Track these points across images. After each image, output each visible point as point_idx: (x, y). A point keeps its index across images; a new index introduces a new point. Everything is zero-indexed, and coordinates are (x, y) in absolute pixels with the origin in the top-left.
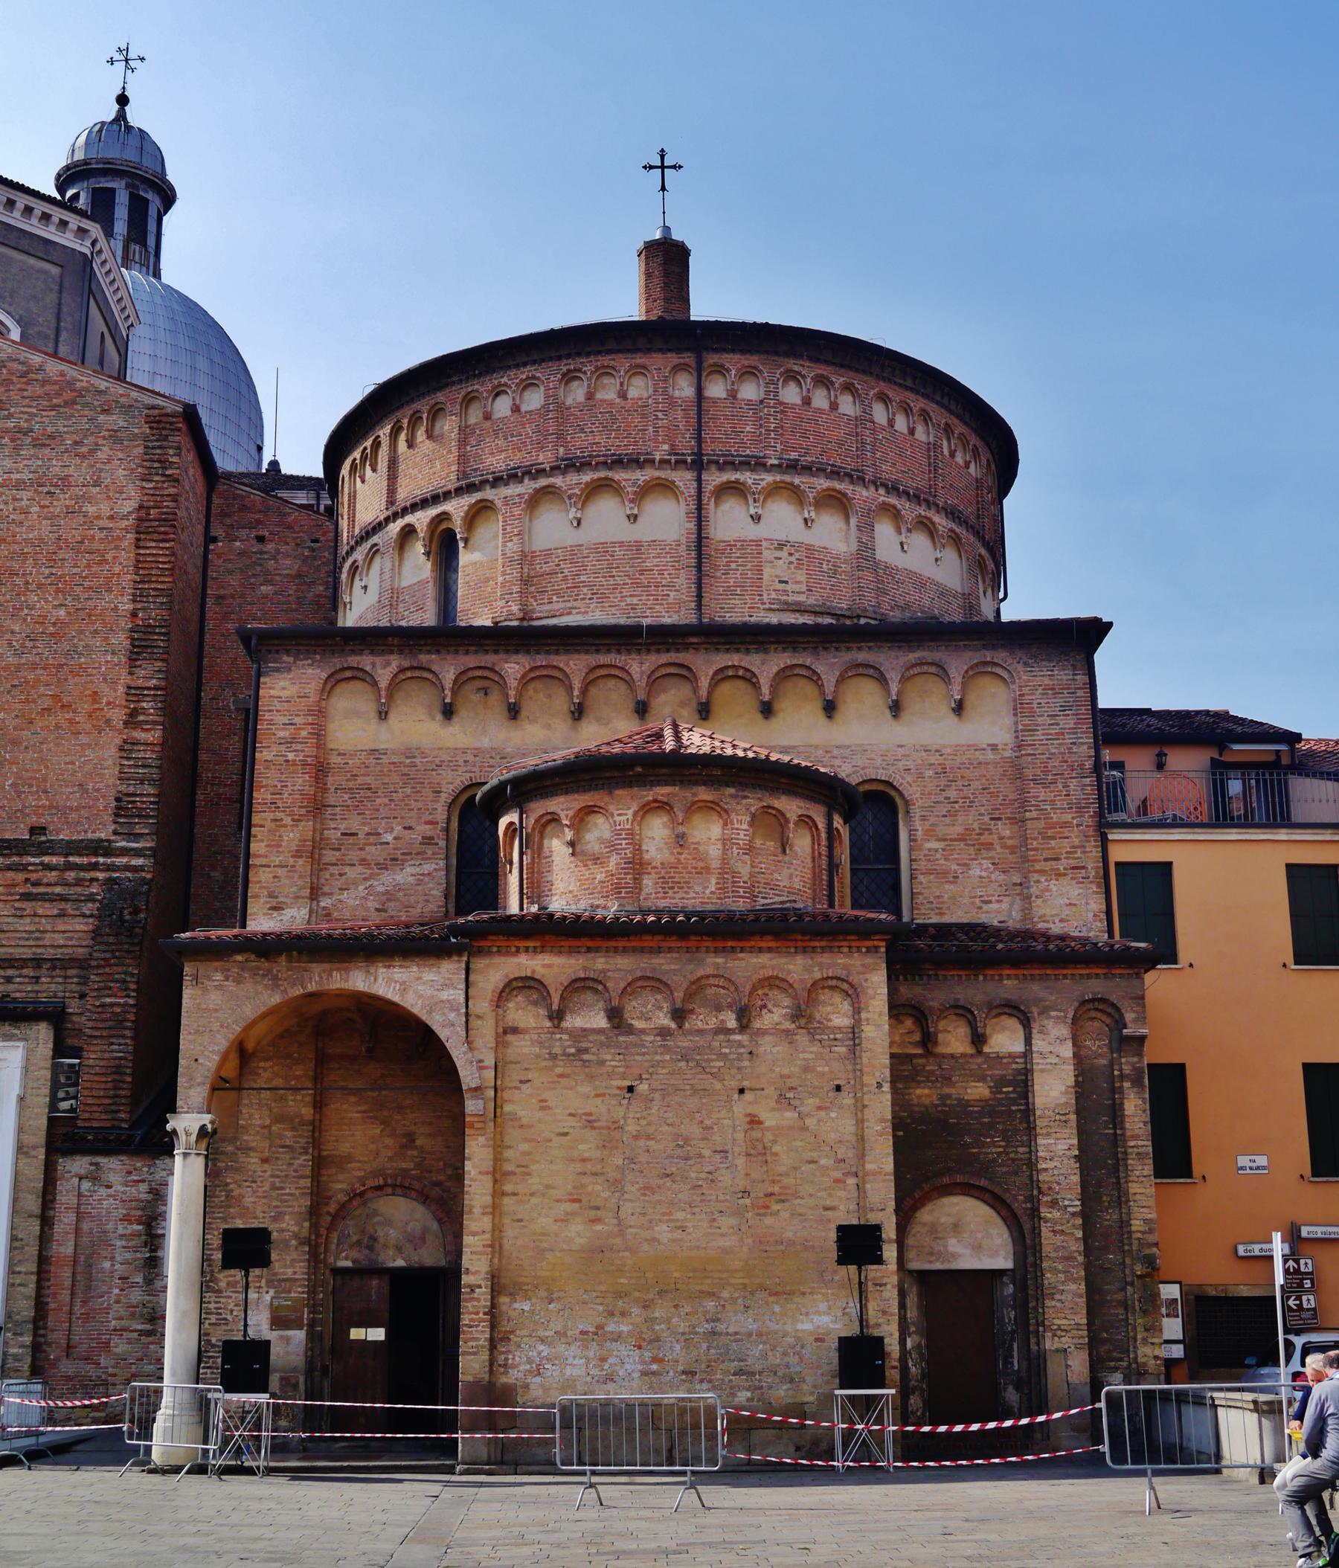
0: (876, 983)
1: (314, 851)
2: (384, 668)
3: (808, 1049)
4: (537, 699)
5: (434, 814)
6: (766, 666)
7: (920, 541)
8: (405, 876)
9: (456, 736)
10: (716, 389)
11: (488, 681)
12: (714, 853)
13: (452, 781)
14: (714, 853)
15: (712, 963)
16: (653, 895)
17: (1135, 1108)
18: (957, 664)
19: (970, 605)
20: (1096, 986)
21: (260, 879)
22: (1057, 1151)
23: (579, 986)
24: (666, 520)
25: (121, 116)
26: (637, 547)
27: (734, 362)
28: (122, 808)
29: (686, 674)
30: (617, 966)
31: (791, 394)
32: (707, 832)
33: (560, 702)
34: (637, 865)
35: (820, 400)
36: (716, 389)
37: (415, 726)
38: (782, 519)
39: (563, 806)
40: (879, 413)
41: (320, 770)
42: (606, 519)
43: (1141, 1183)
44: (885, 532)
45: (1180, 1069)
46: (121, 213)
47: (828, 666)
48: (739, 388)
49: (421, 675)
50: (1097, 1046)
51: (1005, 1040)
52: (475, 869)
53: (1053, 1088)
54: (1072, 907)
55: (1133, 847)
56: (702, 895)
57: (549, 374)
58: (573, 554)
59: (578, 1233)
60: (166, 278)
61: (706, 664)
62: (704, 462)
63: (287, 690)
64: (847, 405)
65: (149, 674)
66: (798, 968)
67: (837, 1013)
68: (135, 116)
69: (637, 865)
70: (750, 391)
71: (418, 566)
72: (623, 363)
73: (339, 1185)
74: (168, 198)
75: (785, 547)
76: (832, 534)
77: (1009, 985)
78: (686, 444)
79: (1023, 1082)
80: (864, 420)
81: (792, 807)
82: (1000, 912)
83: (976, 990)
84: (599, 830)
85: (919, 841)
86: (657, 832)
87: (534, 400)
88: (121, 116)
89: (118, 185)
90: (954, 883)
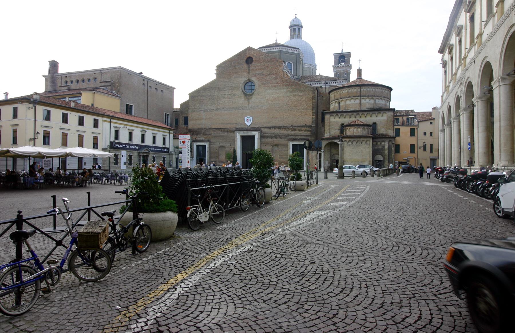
0: (371, 140)
1: (329, 129)
2: (335, 115)
3: (366, 145)
4: (347, 117)
5: (338, 126)
6: (366, 113)
7: (381, 100)
8: (337, 131)
9: (340, 120)
10: (362, 90)
11: (343, 115)
12: (359, 131)
13: (340, 123)
14: (359, 131)
15: (359, 139)
16: (355, 134)
17: (393, 149)
18: (382, 112)
19: (386, 105)
20: (391, 139)
21: (325, 131)
22: (386, 152)
23: (349, 141)
24: (357, 101)
25: (296, 17)
26: (355, 104)
27: (363, 87)
28: (312, 122)
29: (359, 114)
30: (352, 140)
31: (369, 90)
32: (359, 130)
33: (349, 117)
34: (354, 132)
35: (371, 90)
36: (362, 90)
37: (337, 119)
38: (367, 100)
39: (348, 128)
40: (377, 90)
41: (330, 123)
42: (353, 101)
43: (393, 154)
44: (377, 100)
45: (399, 145)
46: (297, 31)
47: (371, 113)
48: (364, 89)
49: (337, 115)
50: (390, 143)
51: (383, 143)
52: (342, 132)
53: (386, 147)
54: (391, 133)
55: (396, 127)
56: (359, 134)
57: (348, 89)
58: (350, 104)
59: (349, 157)
60: (303, 39)
61: (360, 113)
62: (361, 96)
63: (327, 117)
64: (374, 90)
65: (314, 111)
66: (365, 139)
67: (368, 142)
68: (298, 17)
69: (354, 132)
70: (365, 90)
71: (337, 105)
72: (354, 88)
73: (332, 154)
74: (302, 27)
75: (367, 103)
76: (372, 101)
77: (383, 139)
78: (359, 94)
79: (384, 147)
80: (375, 91)
81: (366, 127)
82: (385, 133)
83: (381, 140)
84: (351, 130)
85: (378, 127)
86: (355, 129)
87: (346, 91)
88: (296, 17)
89: (296, 27)
90: (381, 130)
